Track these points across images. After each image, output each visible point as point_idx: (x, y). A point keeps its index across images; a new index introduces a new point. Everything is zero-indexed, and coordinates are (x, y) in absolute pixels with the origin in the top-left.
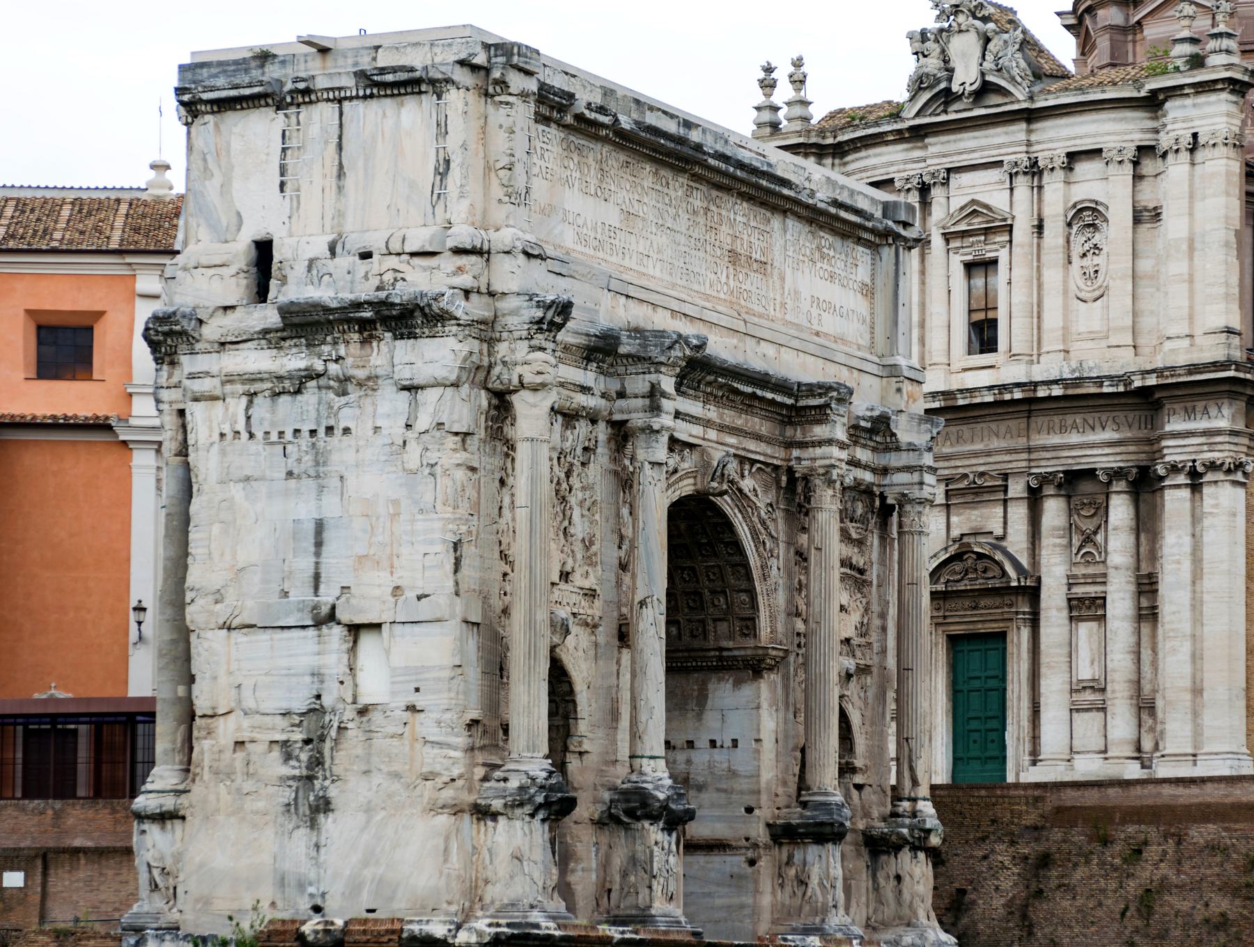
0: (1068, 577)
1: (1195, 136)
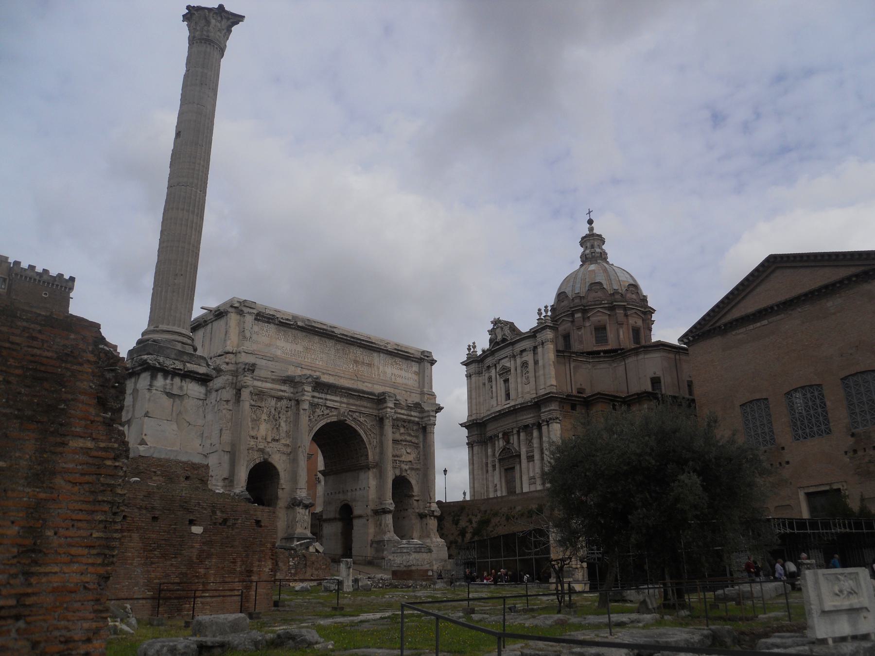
0: (527, 451)
1: (542, 341)
